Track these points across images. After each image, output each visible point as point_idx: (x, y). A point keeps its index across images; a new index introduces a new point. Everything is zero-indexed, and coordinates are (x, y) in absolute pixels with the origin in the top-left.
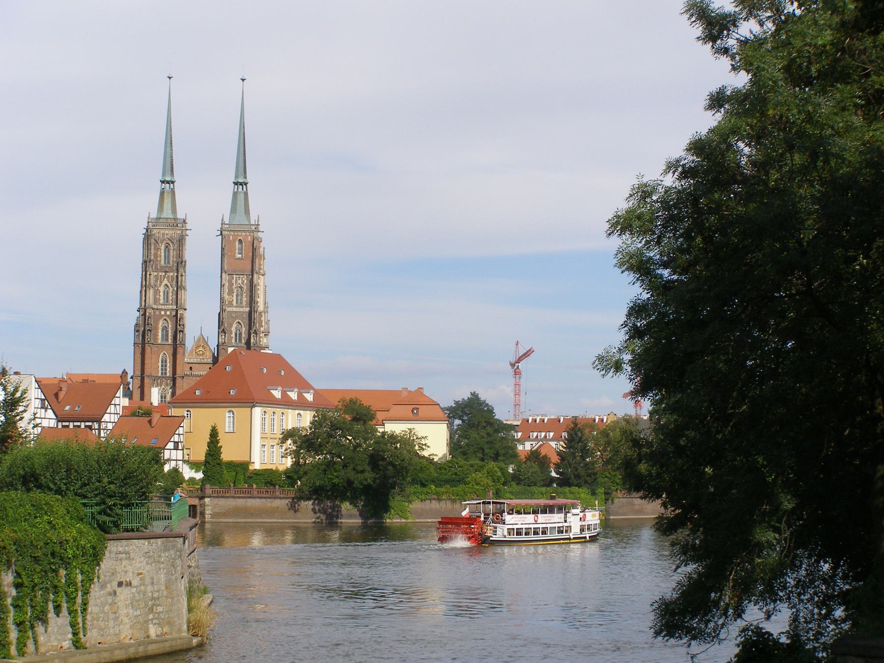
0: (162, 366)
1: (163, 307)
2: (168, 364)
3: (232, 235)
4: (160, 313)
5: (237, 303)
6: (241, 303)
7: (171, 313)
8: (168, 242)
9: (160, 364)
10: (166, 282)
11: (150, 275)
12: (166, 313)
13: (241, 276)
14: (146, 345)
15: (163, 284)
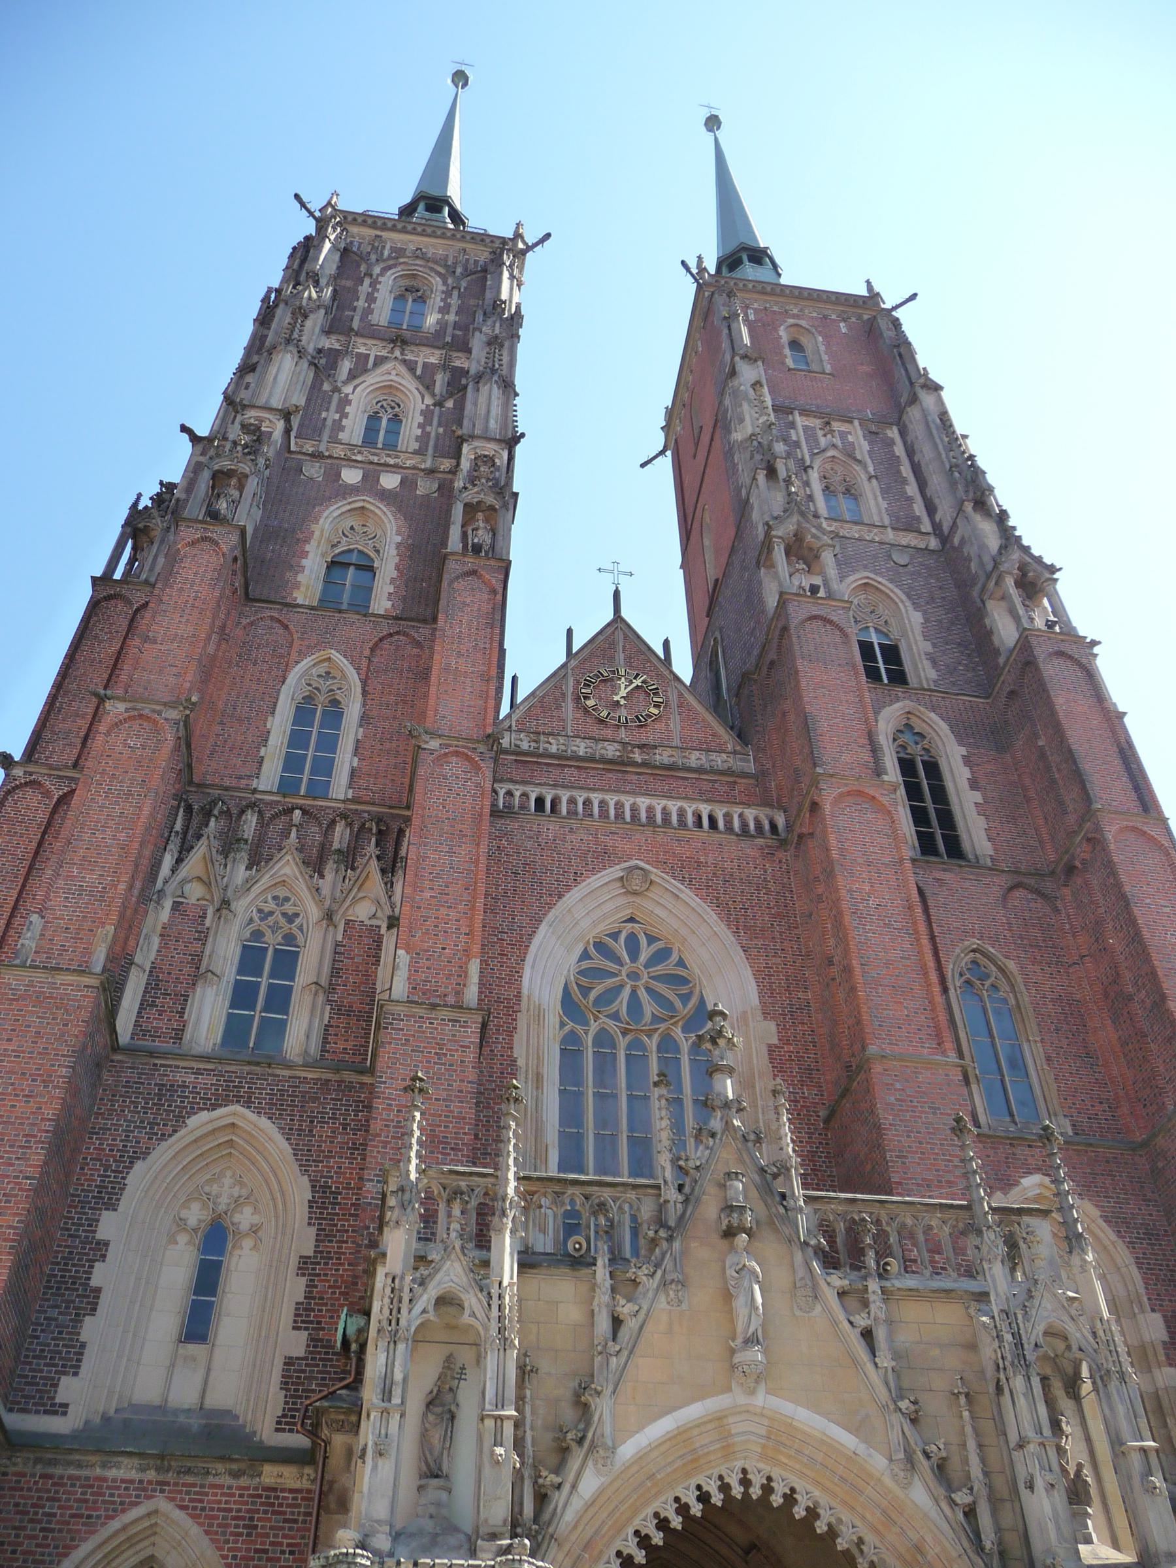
15: (373, 379)
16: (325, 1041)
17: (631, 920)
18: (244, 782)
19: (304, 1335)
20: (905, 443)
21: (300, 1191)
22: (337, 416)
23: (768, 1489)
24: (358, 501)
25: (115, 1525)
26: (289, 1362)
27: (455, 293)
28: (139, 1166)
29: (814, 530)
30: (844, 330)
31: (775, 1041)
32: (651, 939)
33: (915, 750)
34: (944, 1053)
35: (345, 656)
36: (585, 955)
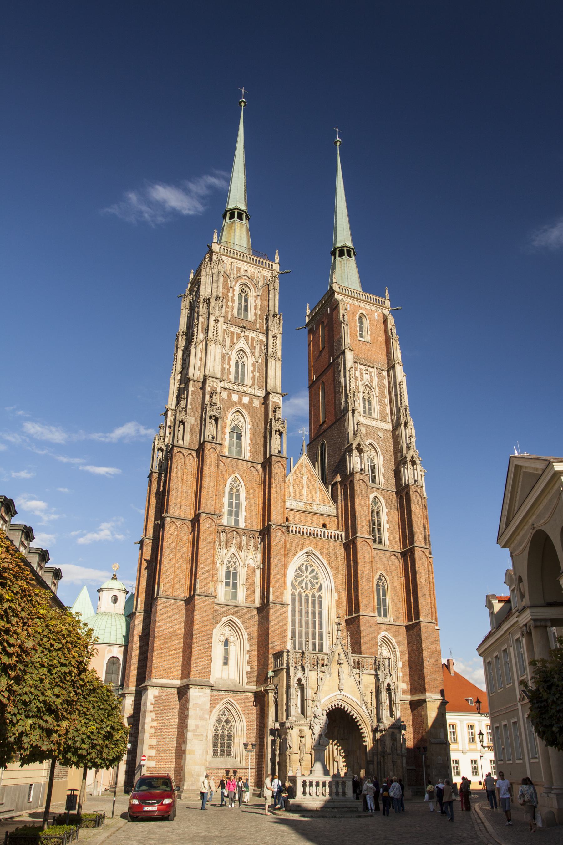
0: (230, 505)
1: (236, 388)
2: (243, 503)
3: (351, 305)
4: (230, 397)
5: (365, 412)
6: (370, 413)
7: (251, 401)
8: (248, 282)
9: (226, 500)
10: (242, 344)
11: (216, 321)
12: (240, 399)
13: (369, 369)
14: (208, 446)
15: (237, 347)
16: (246, 598)
17: (306, 561)
18: (220, 521)
19: (249, 667)
20: (388, 379)
21: (246, 635)
22: (228, 367)
23: (341, 706)
24: (237, 408)
25: (222, 702)
26: (247, 672)
27: (259, 298)
28: (214, 630)
29: (363, 444)
30: (376, 318)
31: (337, 599)
32: (311, 566)
33: (376, 508)
34: (374, 613)
35: (240, 476)
36: (296, 571)
